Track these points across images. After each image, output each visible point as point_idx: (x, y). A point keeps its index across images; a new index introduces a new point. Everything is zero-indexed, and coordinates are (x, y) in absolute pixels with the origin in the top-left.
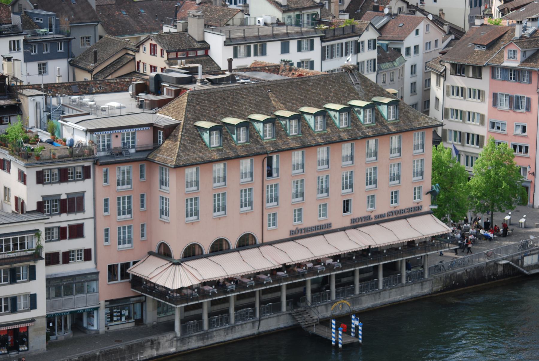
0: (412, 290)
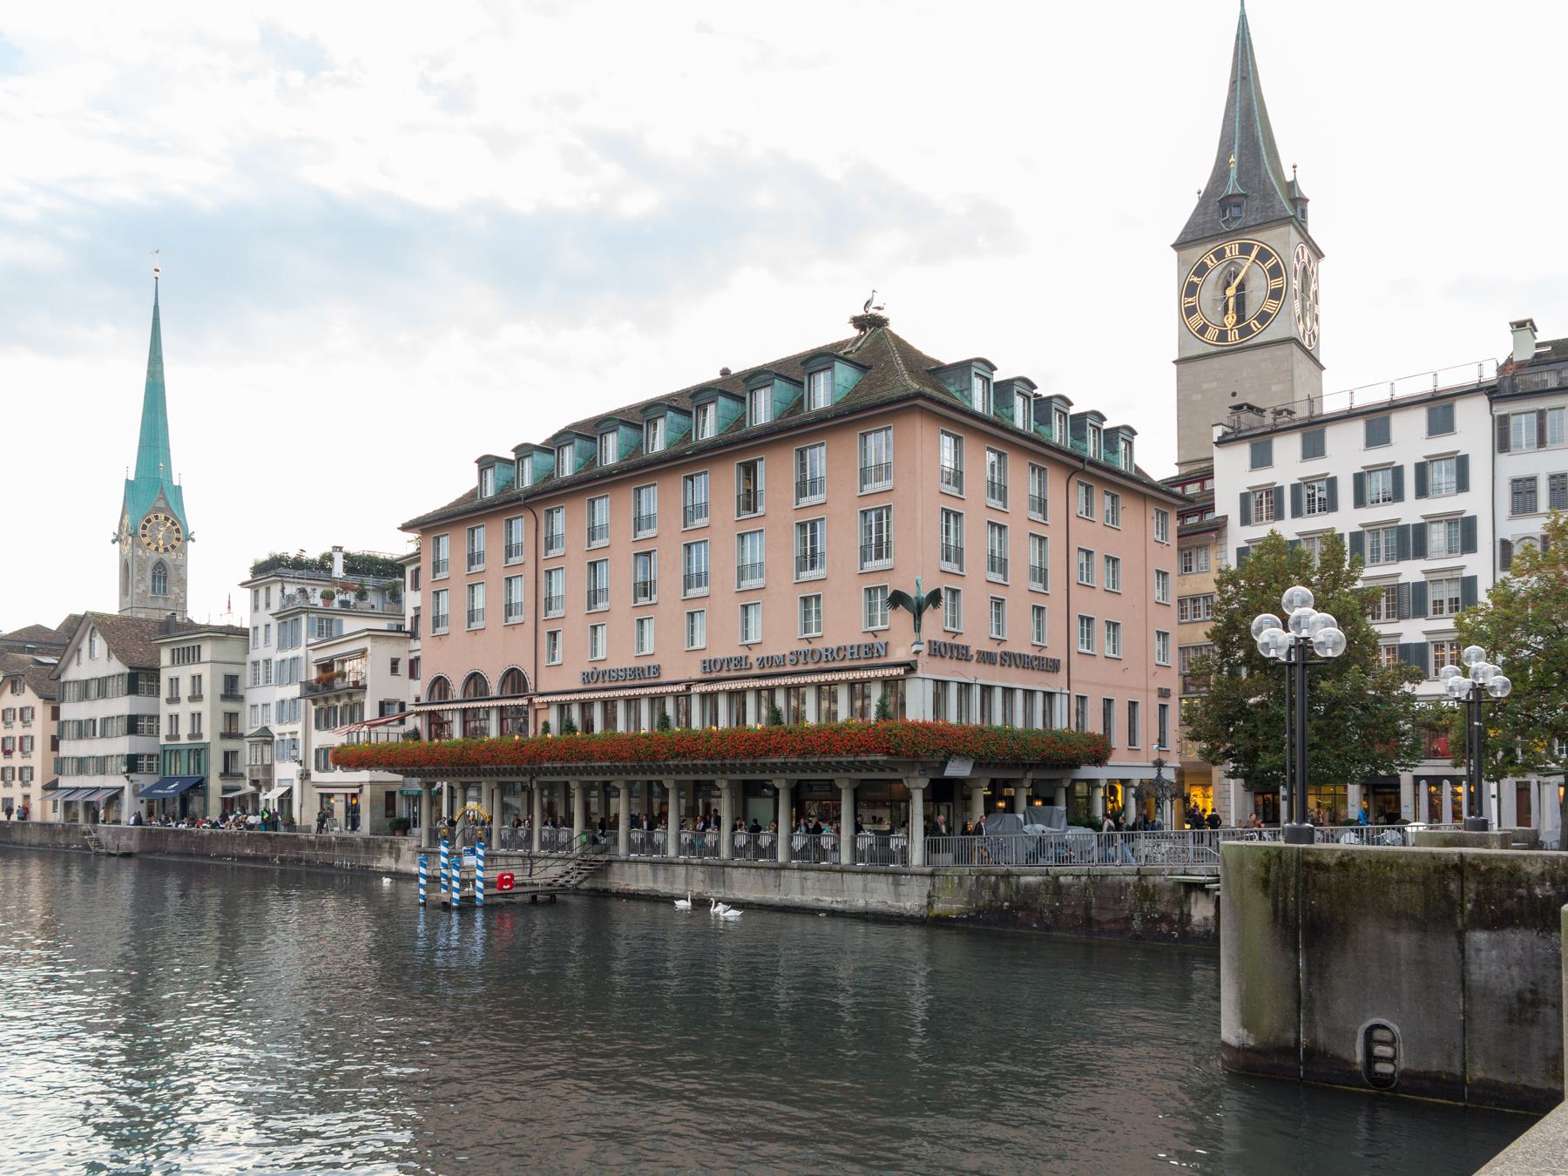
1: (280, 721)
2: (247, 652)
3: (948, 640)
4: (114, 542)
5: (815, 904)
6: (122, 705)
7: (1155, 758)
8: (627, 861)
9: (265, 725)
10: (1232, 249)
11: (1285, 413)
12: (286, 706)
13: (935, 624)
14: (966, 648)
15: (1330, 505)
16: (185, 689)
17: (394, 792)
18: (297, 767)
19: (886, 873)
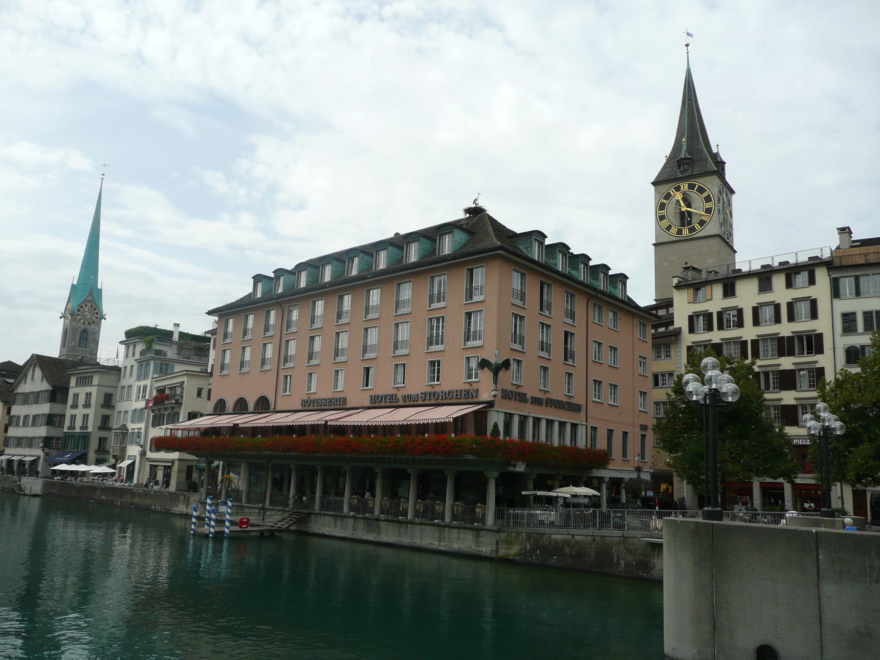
0: (458, 538)
1: (133, 421)
2: (119, 380)
3: (514, 389)
4: (61, 318)
5: (429, 546)
6: (45, 408)
7: (636, 466)
8: (320, 514)
9: (125, 423)
10: (684, 186)
11: (713, 273)
12: (137, 414)
13: (507, 379)
14: (525, 395)
15: (740, 324)
16: (82, 400)
17: (192, 466)
18: (139, 449)
19: (471, 529)
